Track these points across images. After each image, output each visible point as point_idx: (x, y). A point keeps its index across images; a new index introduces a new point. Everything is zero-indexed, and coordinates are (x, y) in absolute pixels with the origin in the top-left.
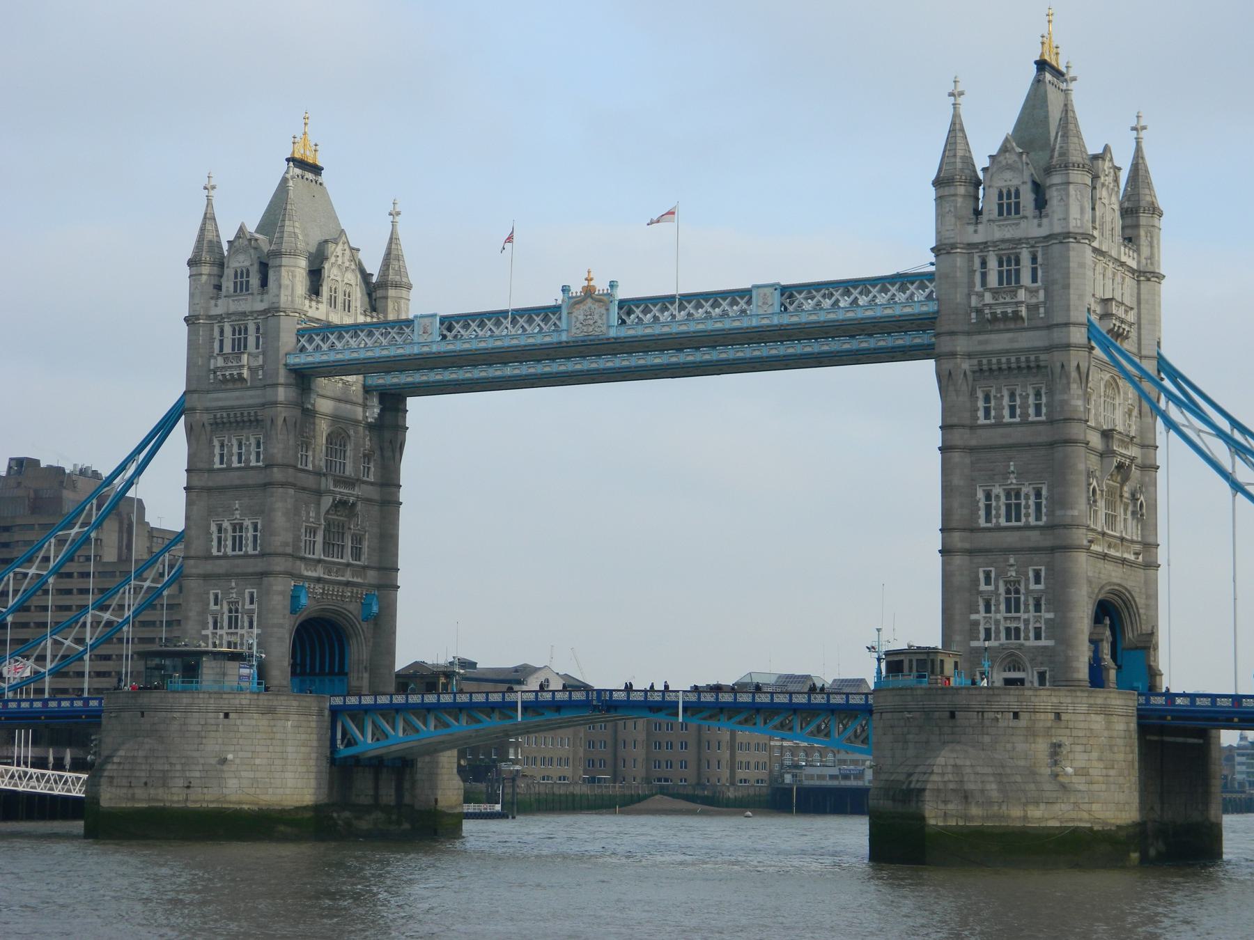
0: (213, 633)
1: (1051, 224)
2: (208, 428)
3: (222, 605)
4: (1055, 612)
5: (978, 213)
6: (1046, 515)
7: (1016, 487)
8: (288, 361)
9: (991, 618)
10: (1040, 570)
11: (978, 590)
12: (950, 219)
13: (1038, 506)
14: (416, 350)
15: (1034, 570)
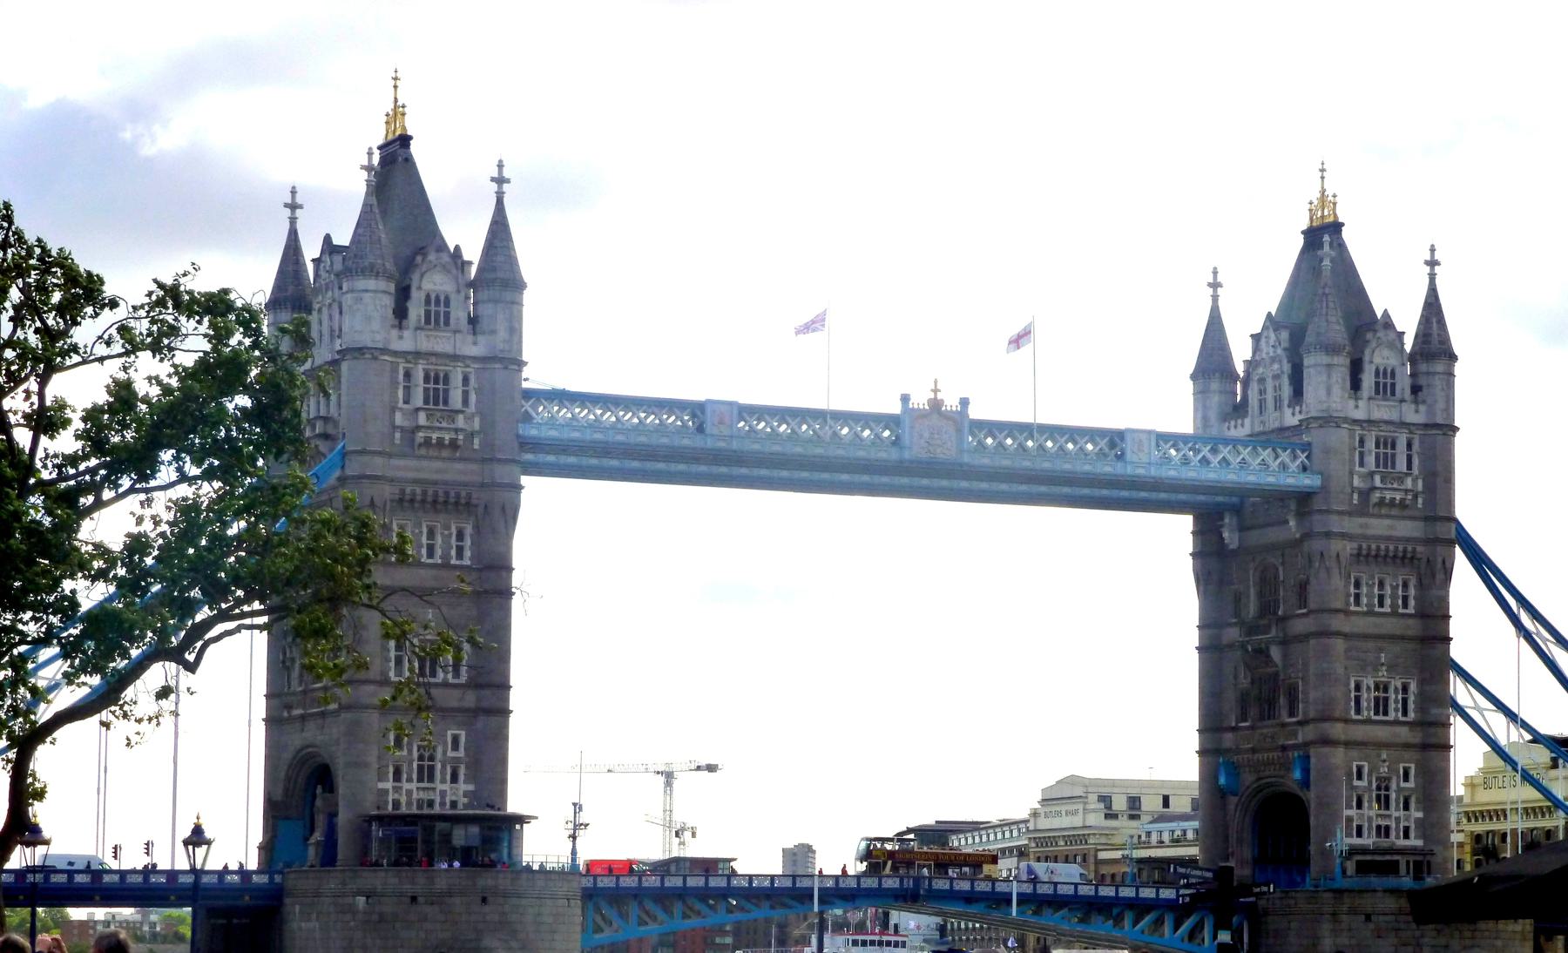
0: (394, 788)
1: (1431, 412)
2: (388, 503)
3: (410, 751)
4: (1425, 810)
5: (1356, 385)
6: (1415, 712)
7: (1386, 680)
8: (521, 432)
9: (1363, 815)
10: (1410, 768)
11: (1352, 784)
12: (1337, 391)
13: (1405, 701)
14: (710, 443)
15: (1404, 768)
